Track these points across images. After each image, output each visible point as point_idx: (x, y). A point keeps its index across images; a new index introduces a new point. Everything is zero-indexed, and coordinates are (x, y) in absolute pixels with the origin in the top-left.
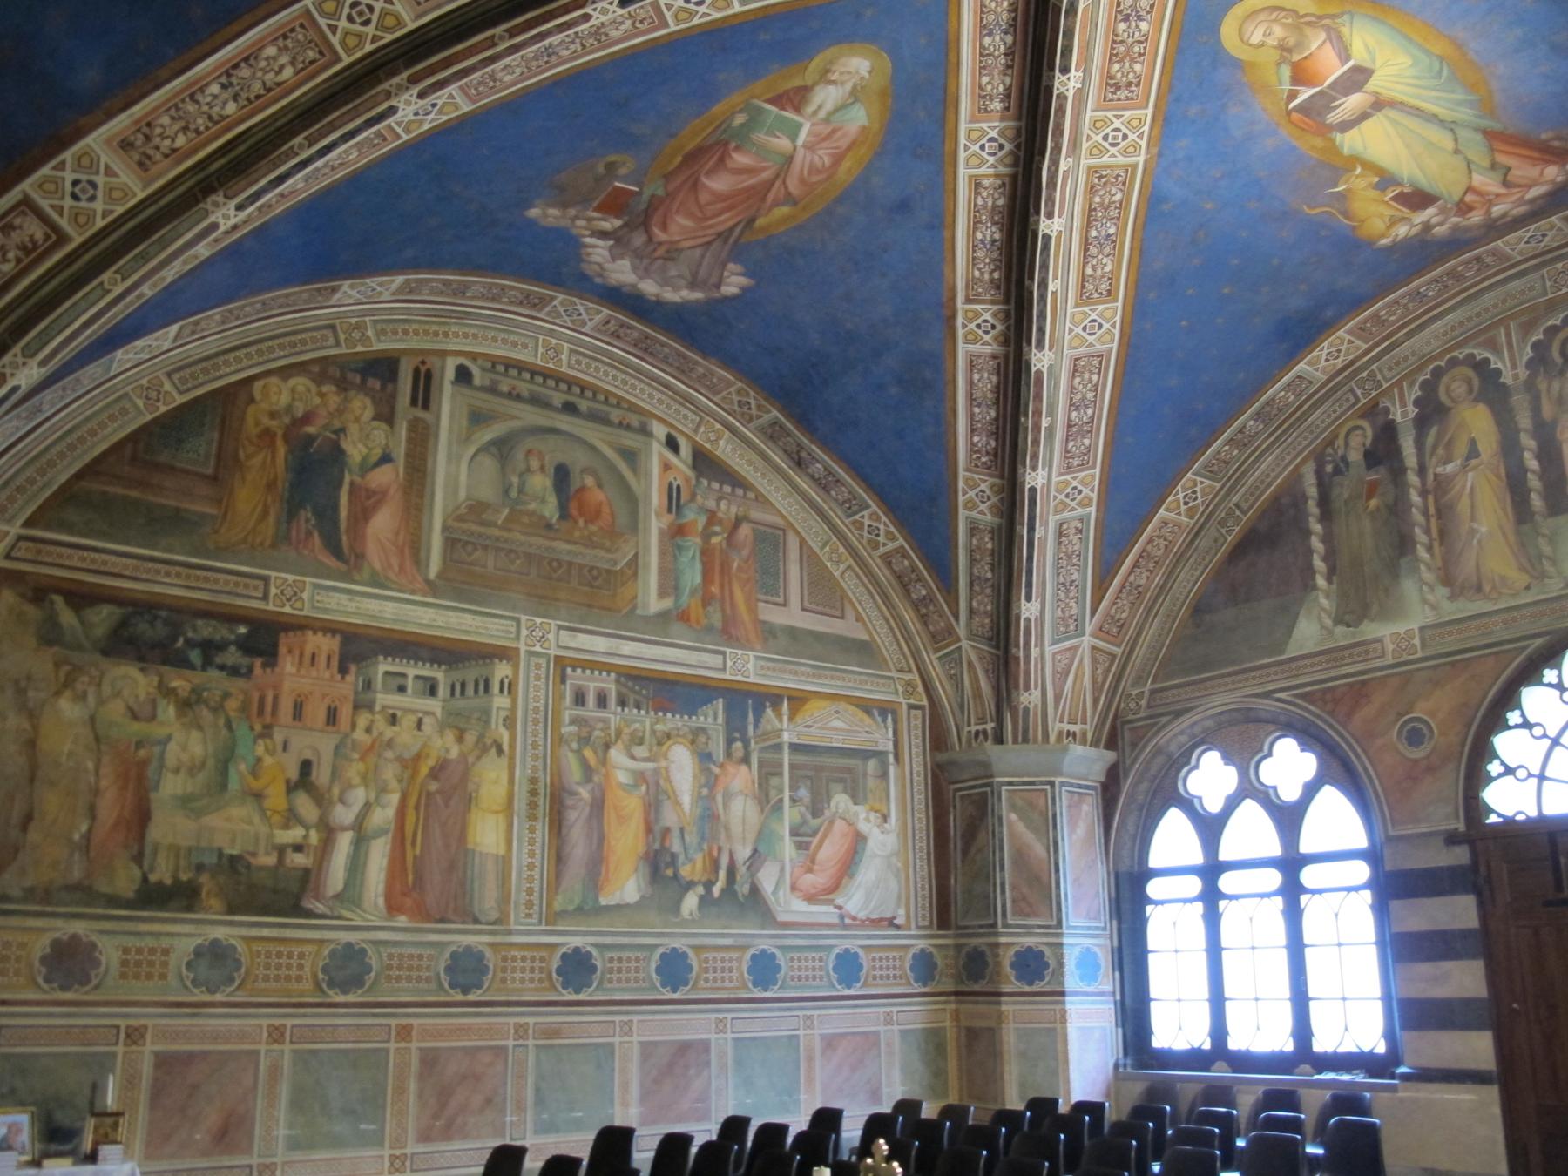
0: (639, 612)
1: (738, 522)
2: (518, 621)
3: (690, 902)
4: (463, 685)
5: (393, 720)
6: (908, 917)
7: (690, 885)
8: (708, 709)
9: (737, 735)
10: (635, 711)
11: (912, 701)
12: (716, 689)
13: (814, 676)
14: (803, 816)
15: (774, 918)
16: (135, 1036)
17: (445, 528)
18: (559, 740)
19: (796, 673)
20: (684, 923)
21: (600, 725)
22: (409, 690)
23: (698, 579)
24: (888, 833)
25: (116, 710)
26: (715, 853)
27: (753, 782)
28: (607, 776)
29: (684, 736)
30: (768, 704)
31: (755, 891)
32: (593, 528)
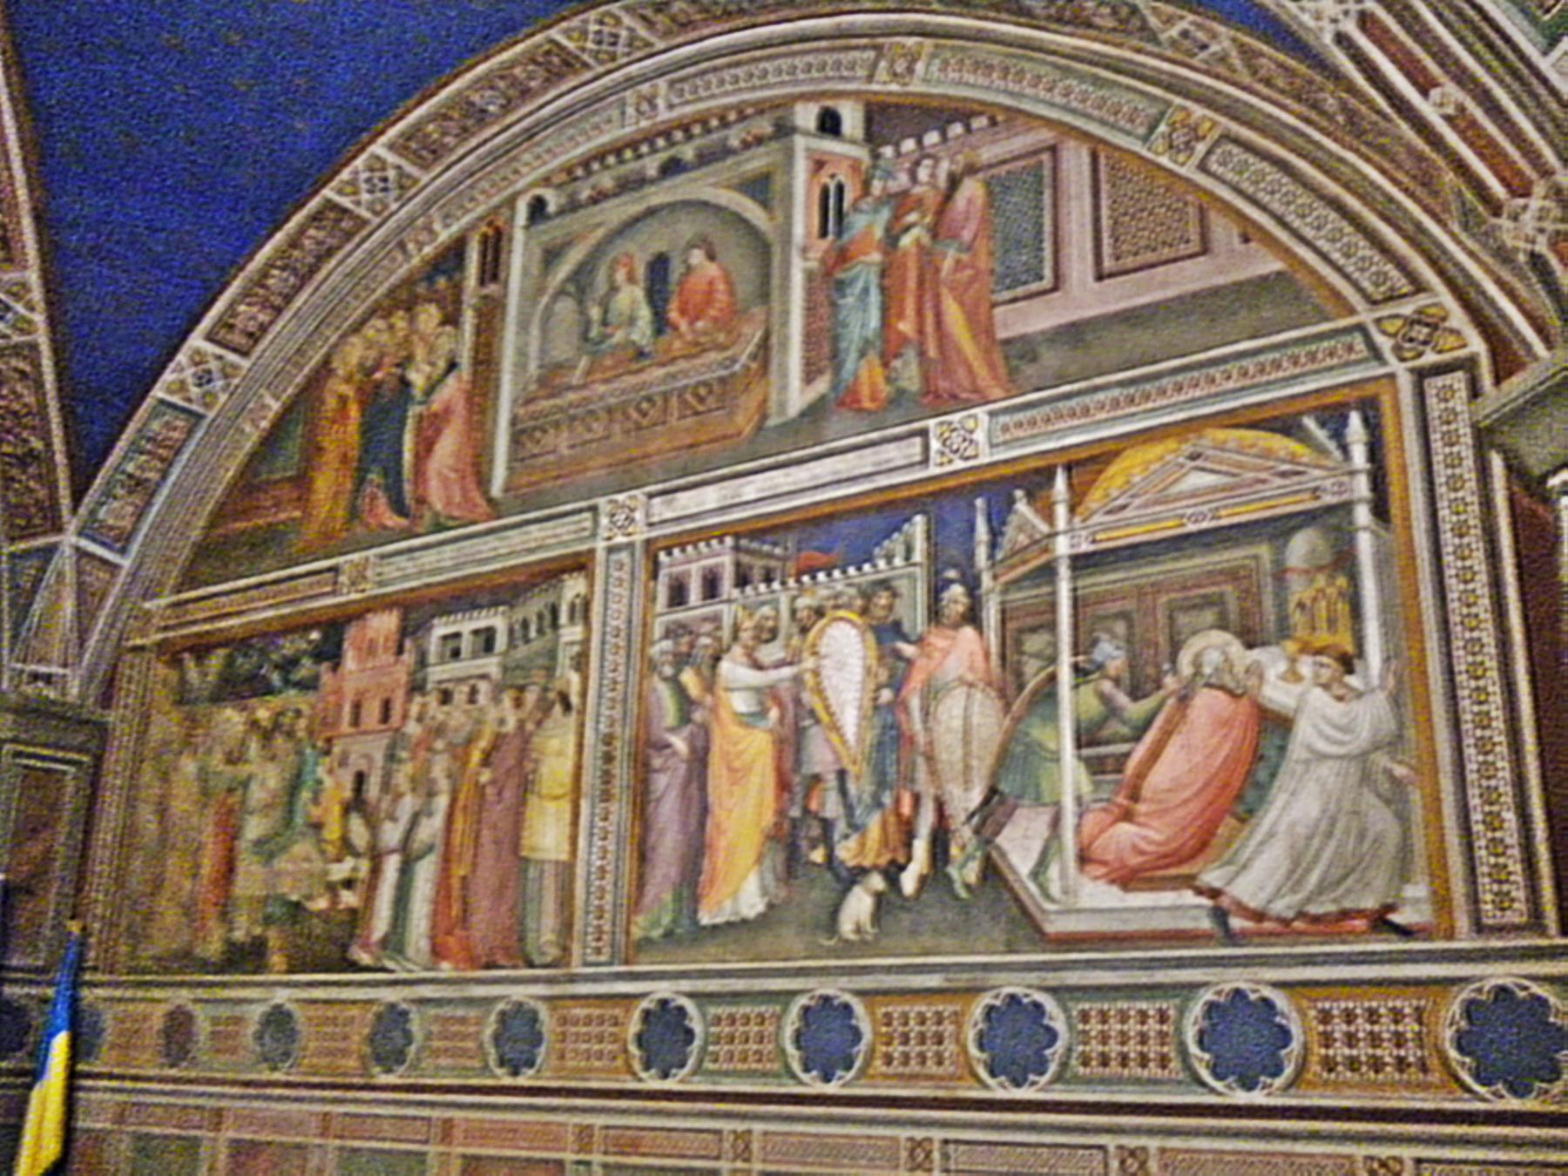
0: (772, 422)
1: (954, 182)
2: (594, 509)
3: (859, 906)
4: (525, 625)
5: (446, 697)
6: (1442, 901)
7: (858, 874)
8: (896, 543)
9: (952, 574)
10: (762, 587)
11: (1430, 358)
12: (909, 501)
13: (1131, 401)
14: (1105, 699)
15: (1039, 930)
16: (217, 1118)
17: (514, 421)
18: (652, 666)
19: (1086, 411)
20: (847, 948)
21: (708, 627)
22: (465, 652)
23: (874, 320)
24: (1359, 695)
25: (216, 761)
26: (906, 809)
27: (987, 655)
28: (714, 710)
29: (848, 606)
30: (1019, 493)
31: (992, 872)
32: (700, 324)
